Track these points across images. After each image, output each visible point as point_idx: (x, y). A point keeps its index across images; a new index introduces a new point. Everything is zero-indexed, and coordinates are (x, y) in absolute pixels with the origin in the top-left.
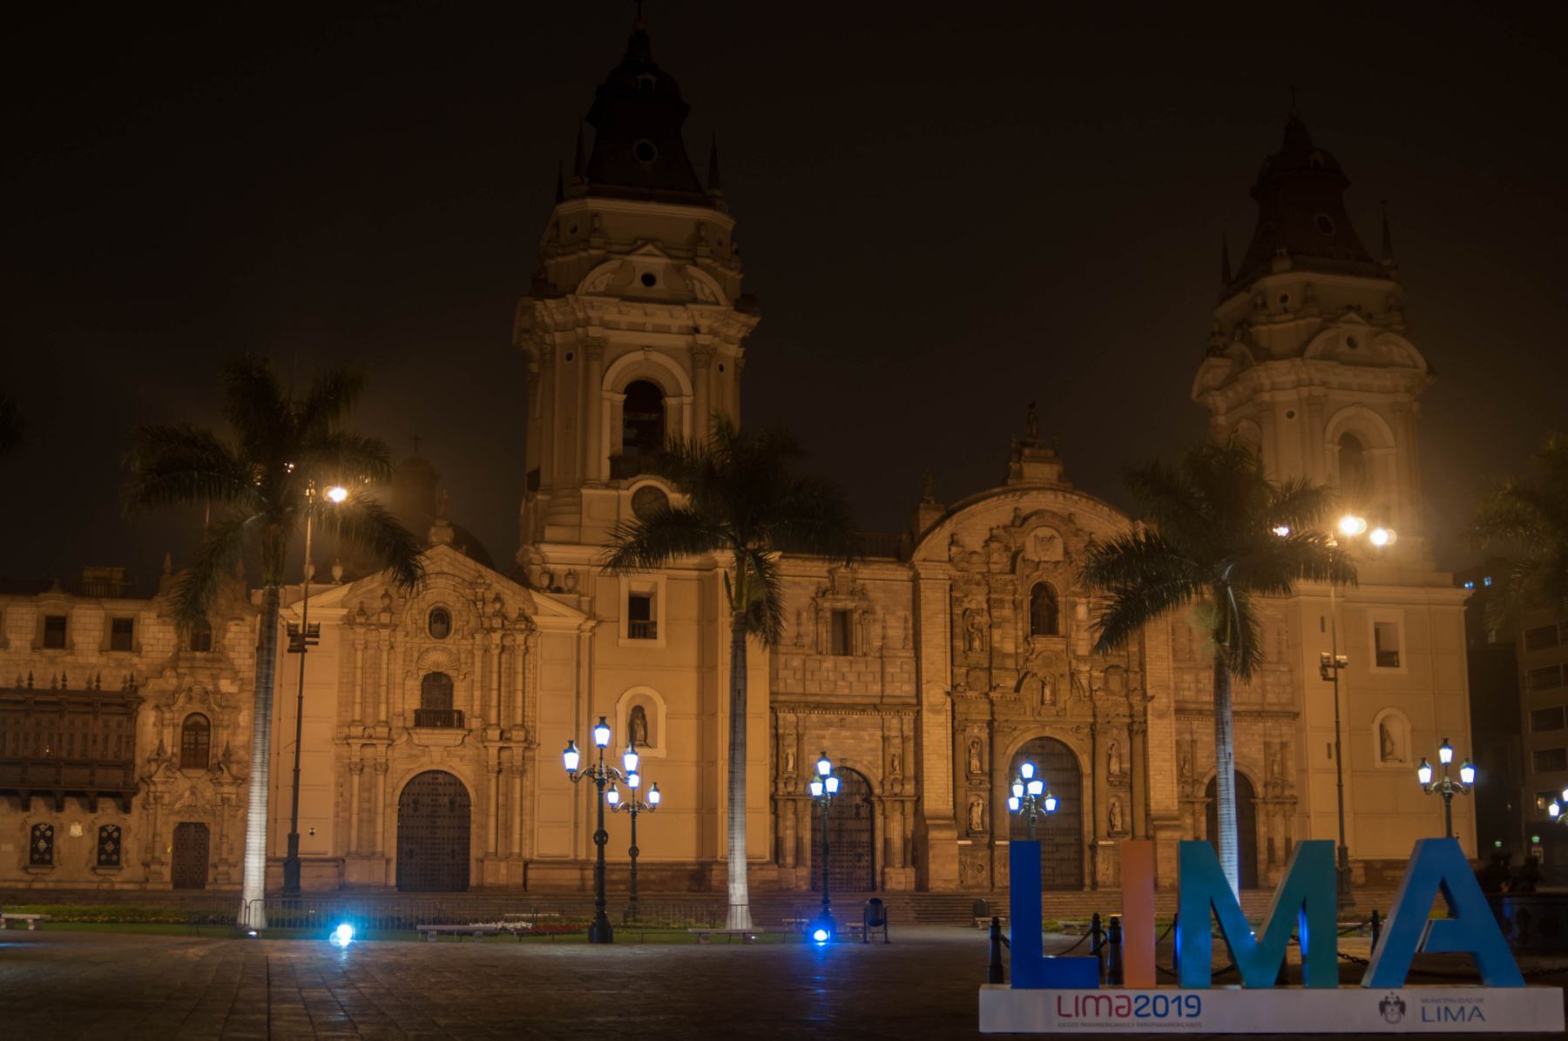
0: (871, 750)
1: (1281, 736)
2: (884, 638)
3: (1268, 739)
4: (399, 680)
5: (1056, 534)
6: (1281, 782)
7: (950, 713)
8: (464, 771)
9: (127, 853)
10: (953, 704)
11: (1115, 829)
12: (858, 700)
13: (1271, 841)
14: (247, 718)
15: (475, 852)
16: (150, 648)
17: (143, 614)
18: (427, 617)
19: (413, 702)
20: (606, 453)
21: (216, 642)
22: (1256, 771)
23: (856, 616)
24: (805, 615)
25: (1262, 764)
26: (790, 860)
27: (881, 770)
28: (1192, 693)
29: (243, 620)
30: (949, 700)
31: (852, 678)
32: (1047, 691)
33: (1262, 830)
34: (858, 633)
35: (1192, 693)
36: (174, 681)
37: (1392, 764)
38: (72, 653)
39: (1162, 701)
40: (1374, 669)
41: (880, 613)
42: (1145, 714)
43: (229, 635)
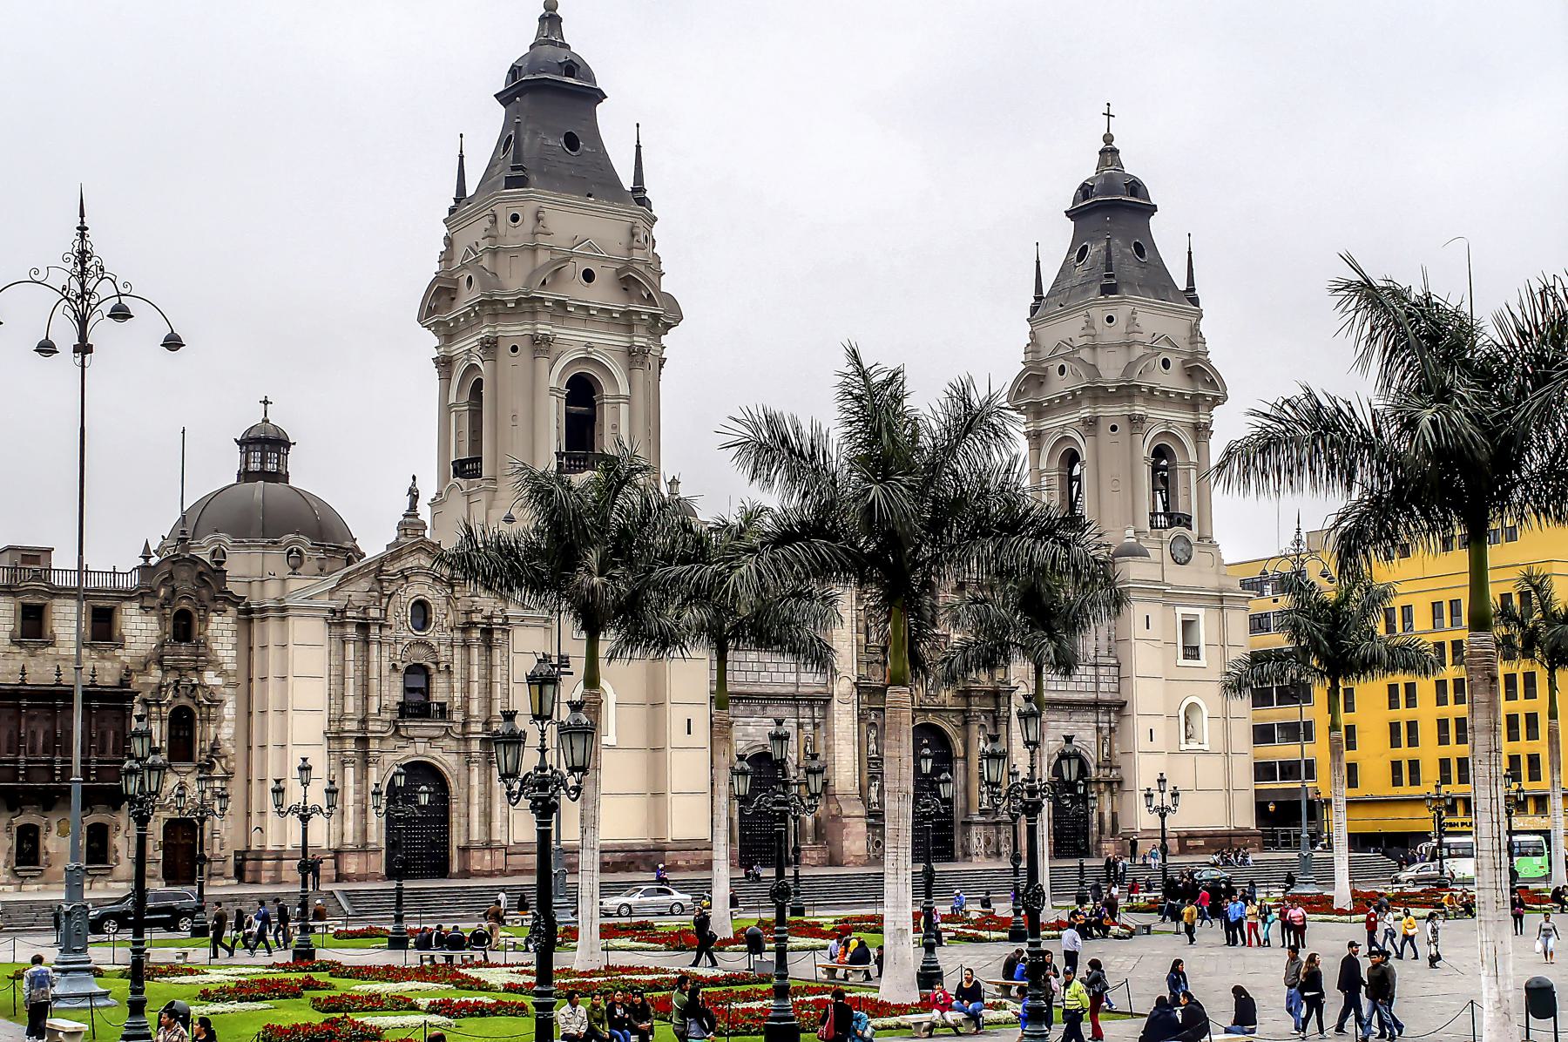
1: (1110, 722)
3: (1100, 725)
6: (1109, 763)
7: (856, 702)
8: (446, 759)
9: (117, 851)
10: (858, 694)
13: (1101, 815)
14: (232, 711)
15: (457, 839)
16: (133, 640)
17: (126, 605)
18: (409, 610)
19: (392, 692)
21: (199, 634)
25: (1094, 746)
27: (796, 755)
29: (225, 611)
30: (855, 690)
31: (772, 667)
36: (159, 673)
37: (1193, 745)
38: (52, 645)
40: (1181, 661)
42: (1009, 703)
43: (211, 626)
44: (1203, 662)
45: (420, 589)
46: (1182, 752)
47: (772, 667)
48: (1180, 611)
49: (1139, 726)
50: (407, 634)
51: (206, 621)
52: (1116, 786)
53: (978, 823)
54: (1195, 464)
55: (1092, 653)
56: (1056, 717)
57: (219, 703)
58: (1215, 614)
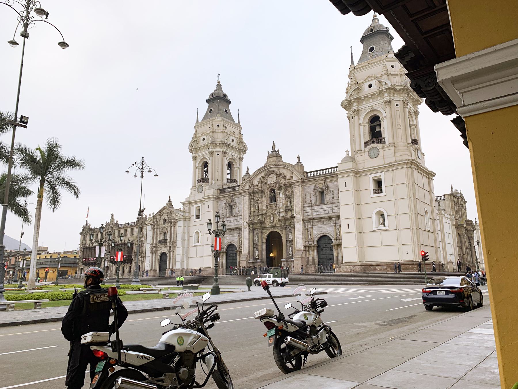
0: (236, 239)
2: (239, 211)
3: (335, 224)
4: (159, 234)
5: (274, 175)
10: (249, 225)
11: (290, 256)
12: (233, 227)
13: (337, 257)
20: (197, 180)
22: (332, 235)
23: (233, 206)
24: (224, 208)
26: (221, 267)
28: (310, 213)
31: (232, 221)
32: (272, 219)
33: (334, 254)
34: (234, 210)
35: (310, 213)
39: (299, 217)
40: (372, 195)
41: (238, 205)
44: (384, 193)
45: (165, 216)
46: (375, 231)
47: (232, 221)
48: (371, 176)
49: (343, 223)
50: (163, 226)
51: (143, 228)
52: (339, 245)
53: (284, 261)
54: (385, 117)
55: (331, 199)
56: (317, 224)
57: (143, 243)
58: (389, 174)
